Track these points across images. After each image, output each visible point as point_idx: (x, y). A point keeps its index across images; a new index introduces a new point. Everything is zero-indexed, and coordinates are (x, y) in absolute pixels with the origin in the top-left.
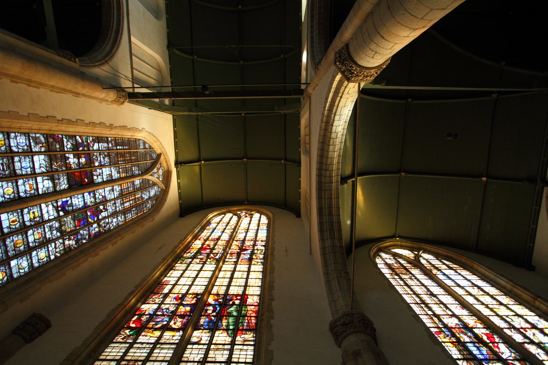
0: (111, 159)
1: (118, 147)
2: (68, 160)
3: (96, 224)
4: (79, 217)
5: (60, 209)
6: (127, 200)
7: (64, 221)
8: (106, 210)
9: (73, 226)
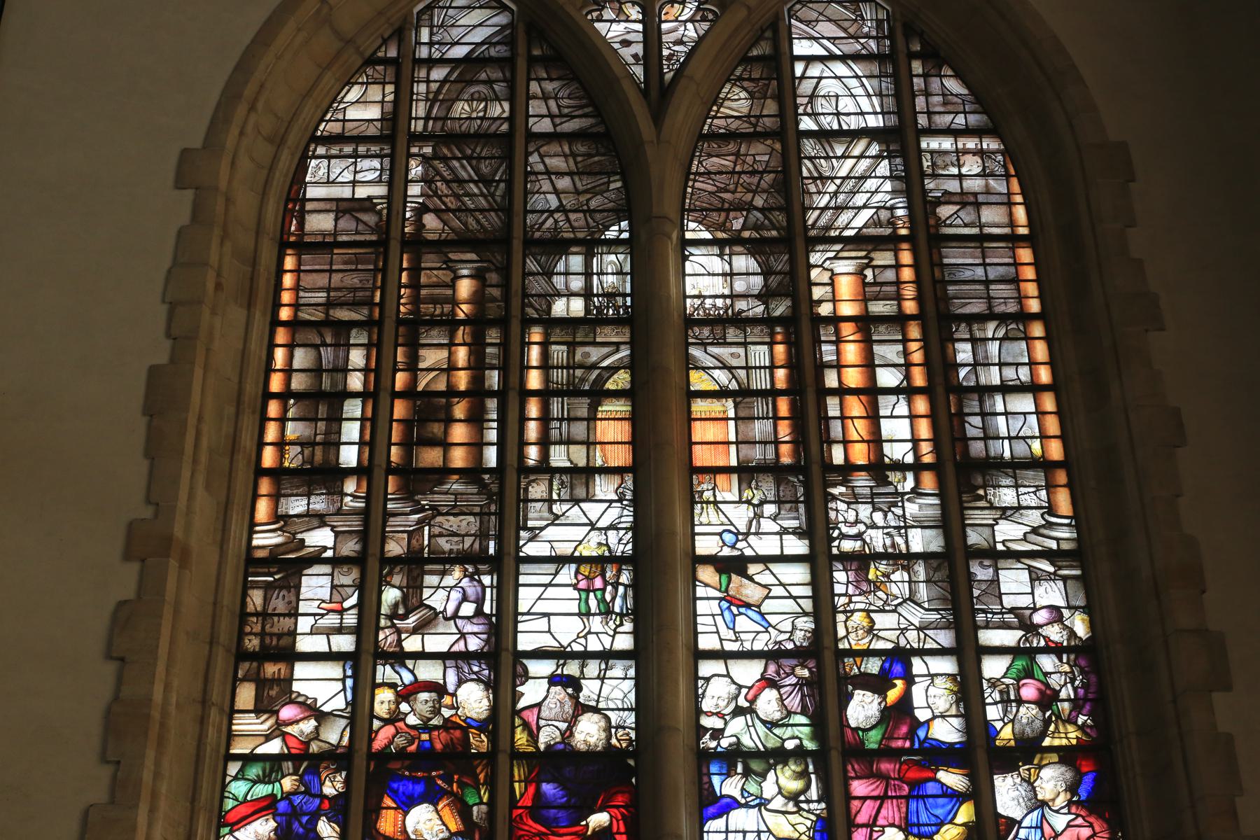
0: (444, 544)
1: (349, 456)
3: (998, 780)
6: (858, 429)
8: (899, 658)
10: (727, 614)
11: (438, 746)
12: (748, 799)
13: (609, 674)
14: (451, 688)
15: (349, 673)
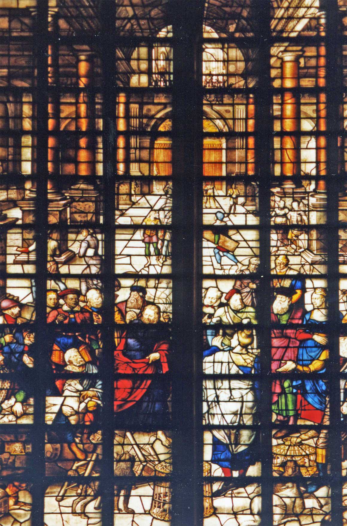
2: (67, 418)
4: (287, 410)
5: (236, 474)
7: (284, 465)
9: (312, 437)
10: (217, 255)
11: (79, 321)
12: (224, 347)
13: (160, 286)
14: (83, 292)
15: (34, 284)
